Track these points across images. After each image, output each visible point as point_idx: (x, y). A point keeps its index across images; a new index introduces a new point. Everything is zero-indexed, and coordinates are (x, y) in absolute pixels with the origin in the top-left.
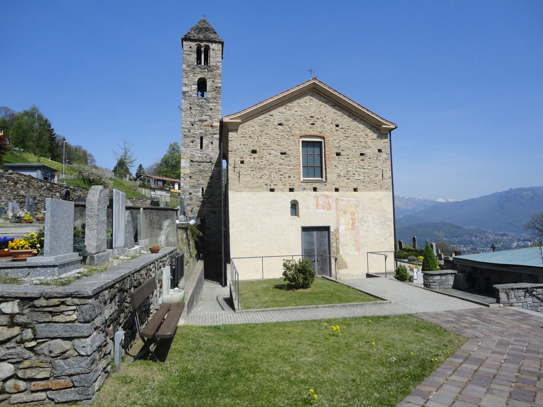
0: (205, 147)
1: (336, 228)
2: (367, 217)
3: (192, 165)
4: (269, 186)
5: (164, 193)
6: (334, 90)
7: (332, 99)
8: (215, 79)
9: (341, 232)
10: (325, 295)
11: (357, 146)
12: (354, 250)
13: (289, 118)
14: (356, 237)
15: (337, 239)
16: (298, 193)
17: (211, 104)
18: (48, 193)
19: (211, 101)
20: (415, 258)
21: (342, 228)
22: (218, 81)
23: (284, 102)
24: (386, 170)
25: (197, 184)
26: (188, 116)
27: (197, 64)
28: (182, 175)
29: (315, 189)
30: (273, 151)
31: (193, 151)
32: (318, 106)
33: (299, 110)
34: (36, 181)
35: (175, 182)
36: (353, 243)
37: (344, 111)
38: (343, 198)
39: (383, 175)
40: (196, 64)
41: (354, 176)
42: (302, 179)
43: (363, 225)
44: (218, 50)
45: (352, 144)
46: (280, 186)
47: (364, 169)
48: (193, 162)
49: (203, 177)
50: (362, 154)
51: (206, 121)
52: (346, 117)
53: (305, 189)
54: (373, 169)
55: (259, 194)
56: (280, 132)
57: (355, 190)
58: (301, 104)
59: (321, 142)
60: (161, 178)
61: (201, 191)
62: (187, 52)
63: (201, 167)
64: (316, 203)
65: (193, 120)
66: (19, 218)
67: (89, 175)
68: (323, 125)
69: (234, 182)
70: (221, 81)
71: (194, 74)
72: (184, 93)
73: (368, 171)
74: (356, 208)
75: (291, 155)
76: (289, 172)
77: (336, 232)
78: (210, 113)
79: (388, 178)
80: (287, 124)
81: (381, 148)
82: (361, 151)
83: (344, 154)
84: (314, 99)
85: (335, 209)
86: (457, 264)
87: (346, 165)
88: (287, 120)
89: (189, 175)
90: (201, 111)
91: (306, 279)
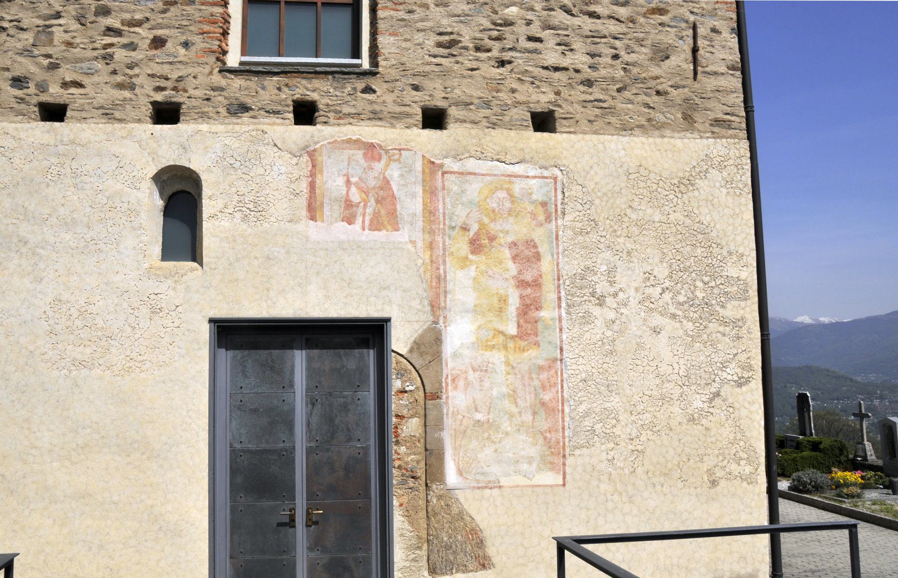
2: (611, 271)
4: (32, 89)
9: (455, 355)
14: (543, 388)
16: (204, 127)
24: (714, 30)
36: (528, 417)
38: (472, 164)
39: (695, 50)
41: (535, 51)
43: (587, 319)
47: (593, 15)
53: (244, 108)
54: (642, 20)
64: (304, 186)
73: (613, 27)
74: (548, 219)
76: (159, 19)
77: (421, 354)
79: (723, 69)
85: (420, 224)
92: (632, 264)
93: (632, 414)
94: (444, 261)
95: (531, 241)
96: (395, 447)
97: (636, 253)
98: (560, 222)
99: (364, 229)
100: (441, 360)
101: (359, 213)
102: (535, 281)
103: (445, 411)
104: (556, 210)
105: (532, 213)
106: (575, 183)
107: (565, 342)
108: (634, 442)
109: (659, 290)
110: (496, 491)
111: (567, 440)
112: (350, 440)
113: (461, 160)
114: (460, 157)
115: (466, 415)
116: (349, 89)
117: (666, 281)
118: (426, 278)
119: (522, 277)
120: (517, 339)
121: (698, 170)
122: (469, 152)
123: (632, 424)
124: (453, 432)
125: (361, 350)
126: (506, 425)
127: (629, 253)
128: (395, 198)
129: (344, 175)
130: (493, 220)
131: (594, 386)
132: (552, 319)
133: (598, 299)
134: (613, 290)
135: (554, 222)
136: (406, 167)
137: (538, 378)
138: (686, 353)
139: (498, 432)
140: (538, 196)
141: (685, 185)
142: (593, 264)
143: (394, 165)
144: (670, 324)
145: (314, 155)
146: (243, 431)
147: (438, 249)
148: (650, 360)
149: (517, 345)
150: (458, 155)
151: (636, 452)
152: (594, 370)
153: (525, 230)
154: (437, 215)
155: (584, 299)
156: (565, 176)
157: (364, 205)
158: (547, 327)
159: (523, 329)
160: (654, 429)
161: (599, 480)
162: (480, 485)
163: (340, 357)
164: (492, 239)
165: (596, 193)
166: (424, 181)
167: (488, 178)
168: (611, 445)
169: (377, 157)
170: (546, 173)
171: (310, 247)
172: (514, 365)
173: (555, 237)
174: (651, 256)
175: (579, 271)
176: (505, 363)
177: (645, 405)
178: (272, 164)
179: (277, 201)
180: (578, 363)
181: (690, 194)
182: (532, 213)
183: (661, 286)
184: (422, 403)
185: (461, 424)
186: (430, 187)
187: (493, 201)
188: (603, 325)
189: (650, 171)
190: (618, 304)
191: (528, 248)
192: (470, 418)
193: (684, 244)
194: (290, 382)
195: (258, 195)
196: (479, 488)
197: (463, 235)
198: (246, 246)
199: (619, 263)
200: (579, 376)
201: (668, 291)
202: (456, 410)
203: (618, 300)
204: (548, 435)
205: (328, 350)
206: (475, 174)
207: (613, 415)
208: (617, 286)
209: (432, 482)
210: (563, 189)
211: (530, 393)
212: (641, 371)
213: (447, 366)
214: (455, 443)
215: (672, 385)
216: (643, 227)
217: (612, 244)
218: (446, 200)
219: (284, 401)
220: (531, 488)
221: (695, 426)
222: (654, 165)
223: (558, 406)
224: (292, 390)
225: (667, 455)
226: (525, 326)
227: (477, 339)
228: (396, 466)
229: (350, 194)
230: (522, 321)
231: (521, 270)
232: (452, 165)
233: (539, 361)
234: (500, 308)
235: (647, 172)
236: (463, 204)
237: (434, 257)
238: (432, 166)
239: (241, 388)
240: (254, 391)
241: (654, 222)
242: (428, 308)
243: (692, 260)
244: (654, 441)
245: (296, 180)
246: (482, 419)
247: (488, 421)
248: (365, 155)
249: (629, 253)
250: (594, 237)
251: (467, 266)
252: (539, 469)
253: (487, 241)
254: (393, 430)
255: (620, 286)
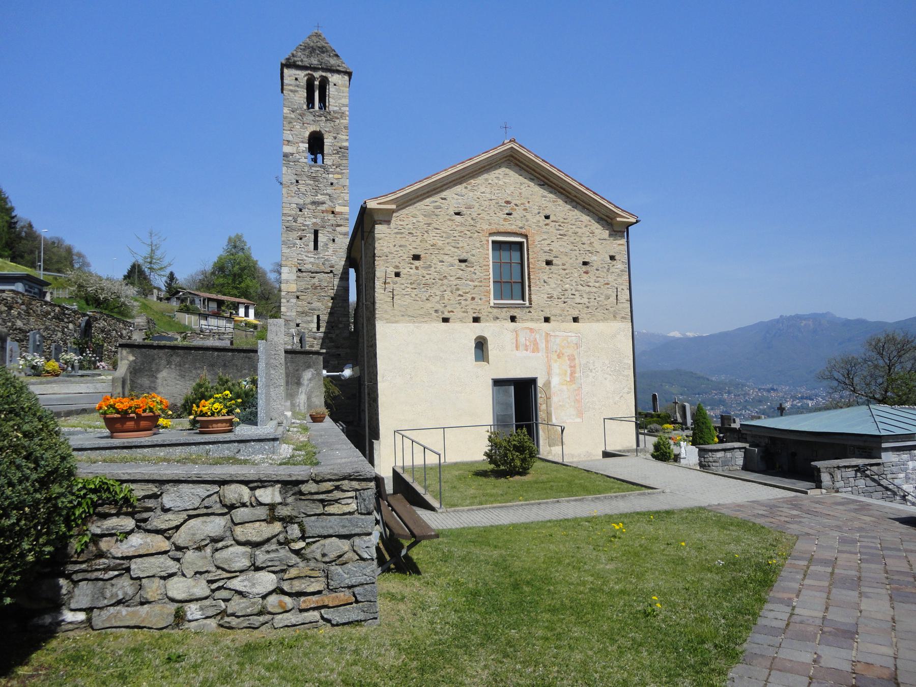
0: (323, 247)
3: (299, 277)
4: (440, 314)
5: (222, 323)
6: (543, 160)
7: (540, 174)
8: (337, 134)
10: (560, 484)
11: (578, 250)
13: (472, 204)
15: (548, 398)
16: (488, 324)
17: (331, 176)
18: (56, 324)
19: (331, 170)
20: (658, 427)
21: (555, 381)
22: (344, 137)
23: (464, 177)
24: (622, 289)
25: (309, 309)
26: (293, 195)
27: (308, 108)
28: (283, 294)
29: (513, 319)
30: (446, 257)
31: (302, 253)
32: (518, 186)
33: (488, 190)
34: (39, 305)
35: (239, 303)
36: (573, 404)
37: (558, 193)
38: (557, 333)
39: (617, 296)
40: (305, 107)
42: (492, 302)
43: (588, 376)
44: (344, 86)
45: (570, 247)
46: (458, 313)
48: (302, 272)
49: (319, 298)
50: (585, 263)
51: (323, 203)
52: (560, 202)
53: (498, 318)
55: (425, 326)
56: (457, 226)
57: (575, 320)
58: (490, 182)
59: (521, 244)
60: (214, 296)
61: (315, 320)
62: (291, 88)
63: (316, 281)
64: (514, 341)
65: (301, 202)
66: (34, 367)
67: (96, 291)
68: (525, 216)
69: (385, 306)
70: (347, 138)
71: (303, 124)
72: (286, 155)
73: (594, 290)
75: (475, 264)
76: (472, 291)
78: (329, 190)
80: (468, 213)
81: (614, 254)
82: (584, 259)
83: (557, 262)
84: (511, 173)
86: (746, 434)
87: (561, 281)
88: (469, 207)
89: (295, 294)
90: (315, 187)
91: (523, 460)
116: (524, 312)
164: (563, 354)
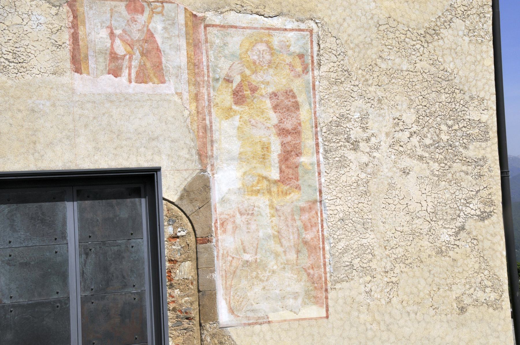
1: (194, 180)
2: (364, 118)
9: (223, 201)
12: (296, 296)
14: (305, 228)
36: (292, 256)
38: (232, 18)
64: (66, 37)
74: (305, 70)
77: (191, 201)
85: (185, 76)
92: (382, 111)
93: (386, 249)
94: (210, 113)
95: (290, 92)
96: (169, 291)
97: (386, 101)
98: (316, 73)
99: (130, 82)
100: (210, 205)
101: (125, 66)
102: (295, 129)
103: (215, 254)
104: (313, 62)
105: (290, 65)
106: (330, 35)
107: (323, 185)
108: (389, 275)
109: (407, 134)
110: (265, 327)
111: (328, 275)
112: (125, 286)
113: (222, 13)
114: (221, 10)
115: (235, 256)
117: (413, 125)
118: (193, 129)
119: (282, 126)
120: (279, 183)
121: (443, 20)
122: (229, 5)
123: (386, 258)
124: (224, 273)
125: (133, 200)
126: (272, 264)
127: (380, 101)
128: (160, 51)
129: (107, 27)
130: (255, 72)
131: (351, 225)
132: (311, 164)
133: (352, 144)
134: (365, 135)
135: (310, 73)
136: (169, 20)
137: (300, 219)
138: (433, 191)
139: (265, 271)
140: (295, 49)
141: (430, 35)
142: (348, 112)
143: (157, 18)
144: (418, 165)
145: (75, 6)
146: (13, 286)
147: (204, 100)
148: (401, 198)
149: (280, 189)
150: (219, 8)
151: (391, 284)
152: (350, 210)
153: (284, 81)
154: (202, 67)
155: (340, 145)
156: (320, 29)
157: (130, 58)
158: (306, 172)
159: (285, 174)
160: (407, 262)
161: (359, 311)
162: (251, 322)
163: (112, 206)
164: (254, 90)
165: (349, 44)
166: (187, 34)
167: (248, 31)
168: (369, 278)
169: (140, 9)
170: (302, 26)
171: (77, 100)
172: (278, 208)
173: (311, 87)
174: (400, 103)
175: (335, 118)
176: (269, 206)
177: (398, 240)
178: (30, 13)
179: (38, 52)
180: (336, 204)
181: (435, 43)
182: (290, 65)
183: (409, 130)
184: (194, 247)
185: (231, 265)
186: (194, 40)
187: (254, 53)
188: (358, 168)
189: (398, 22)
190: (371, 148)
191: (287, 98)
192: (239, 259)
193: (429, 91)
194: (63, 233)
195: (17, 45)
196: (249, 324)
197: (227, 87)
198: (7, 99)
199: (370, 110)
200: (337, 216)
201: (416, 135)
202: (225, 252)
203: (370, 145)
204: (311, 271)
205: (100, 201)
206: (236, 27)
207: (369, 251)
208: (370, 132)
209: (206, 322)
210: (319, 41)
211: (293, 233)
212: (393, 209)
213: (216, 211)
214: (226, 283)
215: (421, 221)
216: (392, 76)
217: (364, 93)
218: (209, 53)
219: (56, 252)
220: (297, 322)
221: (443, 258)
222: (402, 16)
223: (319, 244)
224: (65, 242)
225: (419, 286)
226: (287, 171)
227: (243, 184)
228: (171, 308)
229: (115, 46)
230: (283, 167)
231: (282, 119)
232: (214, 18)
233: (300, 204)
234: (263, 155)
235: (395, 23)
236: (225, 57)
237: (200, 109)
238: (194, 19)
239: (10, 242)
240: (24, 245)
241: (402, 71)
242: (196, 157)
243: (437, 106)
244: (407, 273)
245: (58, 30)
246: (250, 259)
247: (256, 261)
248: (127, 6)
249: (380, 101)
250: (347, 86)
251: (232, 116)
252: (304, 304)
253: (249, 92)
254: (167, 275)
255: (372, 132)
